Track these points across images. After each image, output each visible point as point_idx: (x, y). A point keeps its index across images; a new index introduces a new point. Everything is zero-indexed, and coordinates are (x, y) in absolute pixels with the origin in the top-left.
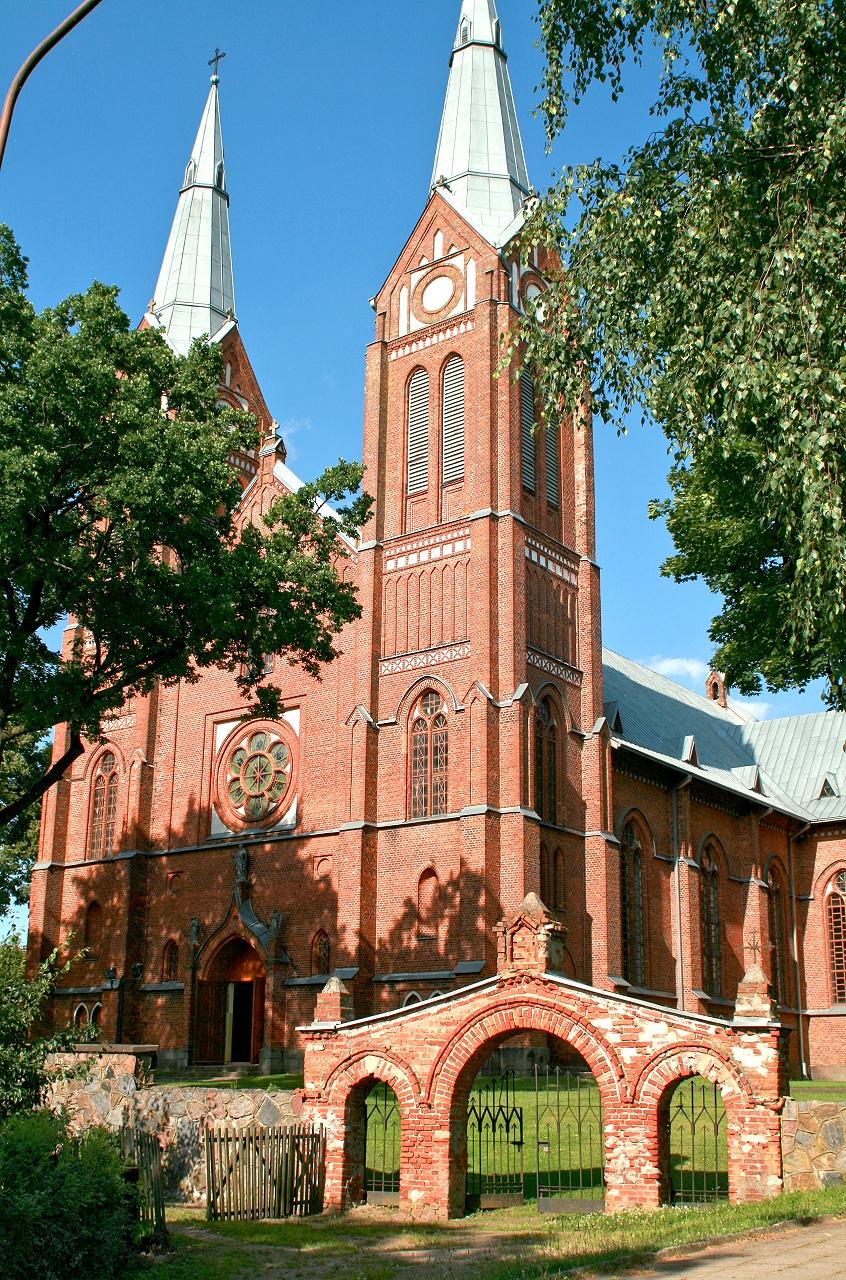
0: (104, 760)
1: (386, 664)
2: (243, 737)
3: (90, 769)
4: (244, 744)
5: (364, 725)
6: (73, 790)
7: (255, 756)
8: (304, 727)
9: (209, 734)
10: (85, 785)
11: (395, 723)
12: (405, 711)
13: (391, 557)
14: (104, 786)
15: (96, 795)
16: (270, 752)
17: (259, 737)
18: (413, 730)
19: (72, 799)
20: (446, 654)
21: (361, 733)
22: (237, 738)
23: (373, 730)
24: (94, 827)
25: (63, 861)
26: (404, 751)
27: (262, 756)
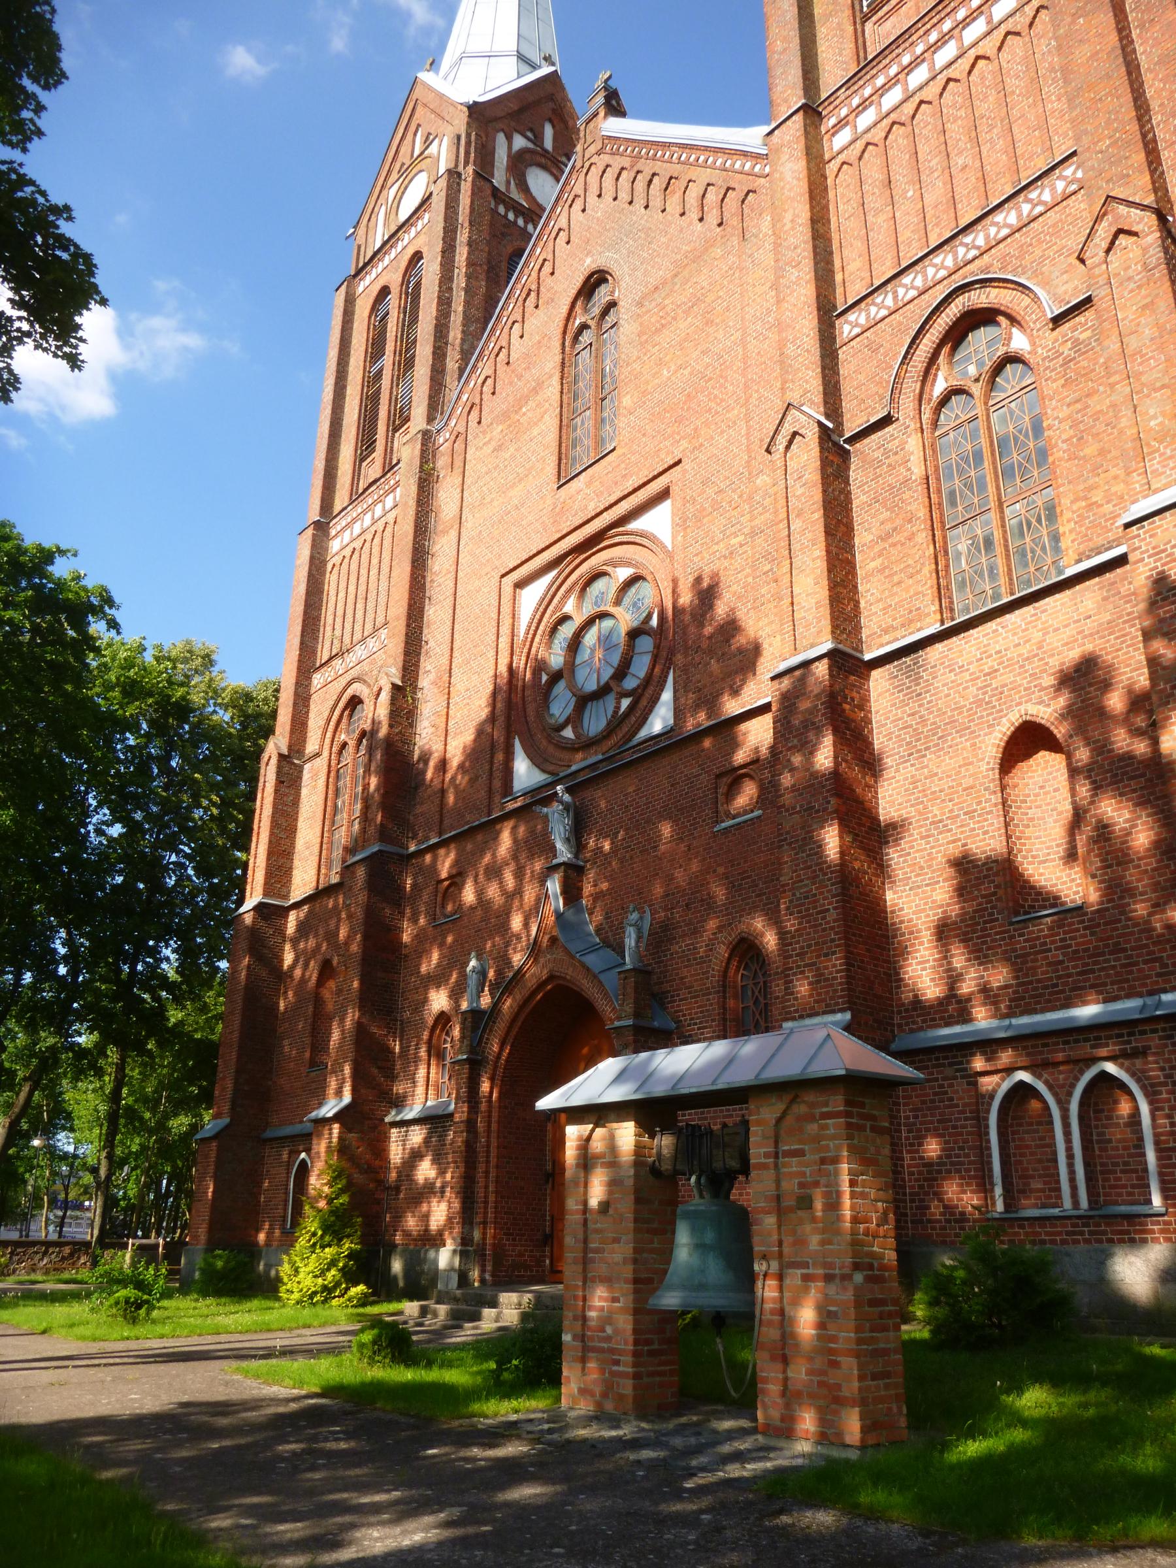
0: (351, 716)
1: (852, 317)
3: (329, 735)
4: (569, 607)
5: (811, 434)
6: (306, 775)
7: (590, 622)
8: (681, 523)
10: (321, 764)
11: (886, 421)
12: (911, 386)
13: (841, 124)
14: (348, 756)
15: (338, 777)
16: (618, 602)
17: (600, 585)
18: (935, 424)
19: (304, 792)
20: (1009, 217)
21: (807, 456)
22: (555, 601)
23: (835, 452)
24: (332, 832)
25: (286, 897)
26: (918, 471)
27: (603, 615)
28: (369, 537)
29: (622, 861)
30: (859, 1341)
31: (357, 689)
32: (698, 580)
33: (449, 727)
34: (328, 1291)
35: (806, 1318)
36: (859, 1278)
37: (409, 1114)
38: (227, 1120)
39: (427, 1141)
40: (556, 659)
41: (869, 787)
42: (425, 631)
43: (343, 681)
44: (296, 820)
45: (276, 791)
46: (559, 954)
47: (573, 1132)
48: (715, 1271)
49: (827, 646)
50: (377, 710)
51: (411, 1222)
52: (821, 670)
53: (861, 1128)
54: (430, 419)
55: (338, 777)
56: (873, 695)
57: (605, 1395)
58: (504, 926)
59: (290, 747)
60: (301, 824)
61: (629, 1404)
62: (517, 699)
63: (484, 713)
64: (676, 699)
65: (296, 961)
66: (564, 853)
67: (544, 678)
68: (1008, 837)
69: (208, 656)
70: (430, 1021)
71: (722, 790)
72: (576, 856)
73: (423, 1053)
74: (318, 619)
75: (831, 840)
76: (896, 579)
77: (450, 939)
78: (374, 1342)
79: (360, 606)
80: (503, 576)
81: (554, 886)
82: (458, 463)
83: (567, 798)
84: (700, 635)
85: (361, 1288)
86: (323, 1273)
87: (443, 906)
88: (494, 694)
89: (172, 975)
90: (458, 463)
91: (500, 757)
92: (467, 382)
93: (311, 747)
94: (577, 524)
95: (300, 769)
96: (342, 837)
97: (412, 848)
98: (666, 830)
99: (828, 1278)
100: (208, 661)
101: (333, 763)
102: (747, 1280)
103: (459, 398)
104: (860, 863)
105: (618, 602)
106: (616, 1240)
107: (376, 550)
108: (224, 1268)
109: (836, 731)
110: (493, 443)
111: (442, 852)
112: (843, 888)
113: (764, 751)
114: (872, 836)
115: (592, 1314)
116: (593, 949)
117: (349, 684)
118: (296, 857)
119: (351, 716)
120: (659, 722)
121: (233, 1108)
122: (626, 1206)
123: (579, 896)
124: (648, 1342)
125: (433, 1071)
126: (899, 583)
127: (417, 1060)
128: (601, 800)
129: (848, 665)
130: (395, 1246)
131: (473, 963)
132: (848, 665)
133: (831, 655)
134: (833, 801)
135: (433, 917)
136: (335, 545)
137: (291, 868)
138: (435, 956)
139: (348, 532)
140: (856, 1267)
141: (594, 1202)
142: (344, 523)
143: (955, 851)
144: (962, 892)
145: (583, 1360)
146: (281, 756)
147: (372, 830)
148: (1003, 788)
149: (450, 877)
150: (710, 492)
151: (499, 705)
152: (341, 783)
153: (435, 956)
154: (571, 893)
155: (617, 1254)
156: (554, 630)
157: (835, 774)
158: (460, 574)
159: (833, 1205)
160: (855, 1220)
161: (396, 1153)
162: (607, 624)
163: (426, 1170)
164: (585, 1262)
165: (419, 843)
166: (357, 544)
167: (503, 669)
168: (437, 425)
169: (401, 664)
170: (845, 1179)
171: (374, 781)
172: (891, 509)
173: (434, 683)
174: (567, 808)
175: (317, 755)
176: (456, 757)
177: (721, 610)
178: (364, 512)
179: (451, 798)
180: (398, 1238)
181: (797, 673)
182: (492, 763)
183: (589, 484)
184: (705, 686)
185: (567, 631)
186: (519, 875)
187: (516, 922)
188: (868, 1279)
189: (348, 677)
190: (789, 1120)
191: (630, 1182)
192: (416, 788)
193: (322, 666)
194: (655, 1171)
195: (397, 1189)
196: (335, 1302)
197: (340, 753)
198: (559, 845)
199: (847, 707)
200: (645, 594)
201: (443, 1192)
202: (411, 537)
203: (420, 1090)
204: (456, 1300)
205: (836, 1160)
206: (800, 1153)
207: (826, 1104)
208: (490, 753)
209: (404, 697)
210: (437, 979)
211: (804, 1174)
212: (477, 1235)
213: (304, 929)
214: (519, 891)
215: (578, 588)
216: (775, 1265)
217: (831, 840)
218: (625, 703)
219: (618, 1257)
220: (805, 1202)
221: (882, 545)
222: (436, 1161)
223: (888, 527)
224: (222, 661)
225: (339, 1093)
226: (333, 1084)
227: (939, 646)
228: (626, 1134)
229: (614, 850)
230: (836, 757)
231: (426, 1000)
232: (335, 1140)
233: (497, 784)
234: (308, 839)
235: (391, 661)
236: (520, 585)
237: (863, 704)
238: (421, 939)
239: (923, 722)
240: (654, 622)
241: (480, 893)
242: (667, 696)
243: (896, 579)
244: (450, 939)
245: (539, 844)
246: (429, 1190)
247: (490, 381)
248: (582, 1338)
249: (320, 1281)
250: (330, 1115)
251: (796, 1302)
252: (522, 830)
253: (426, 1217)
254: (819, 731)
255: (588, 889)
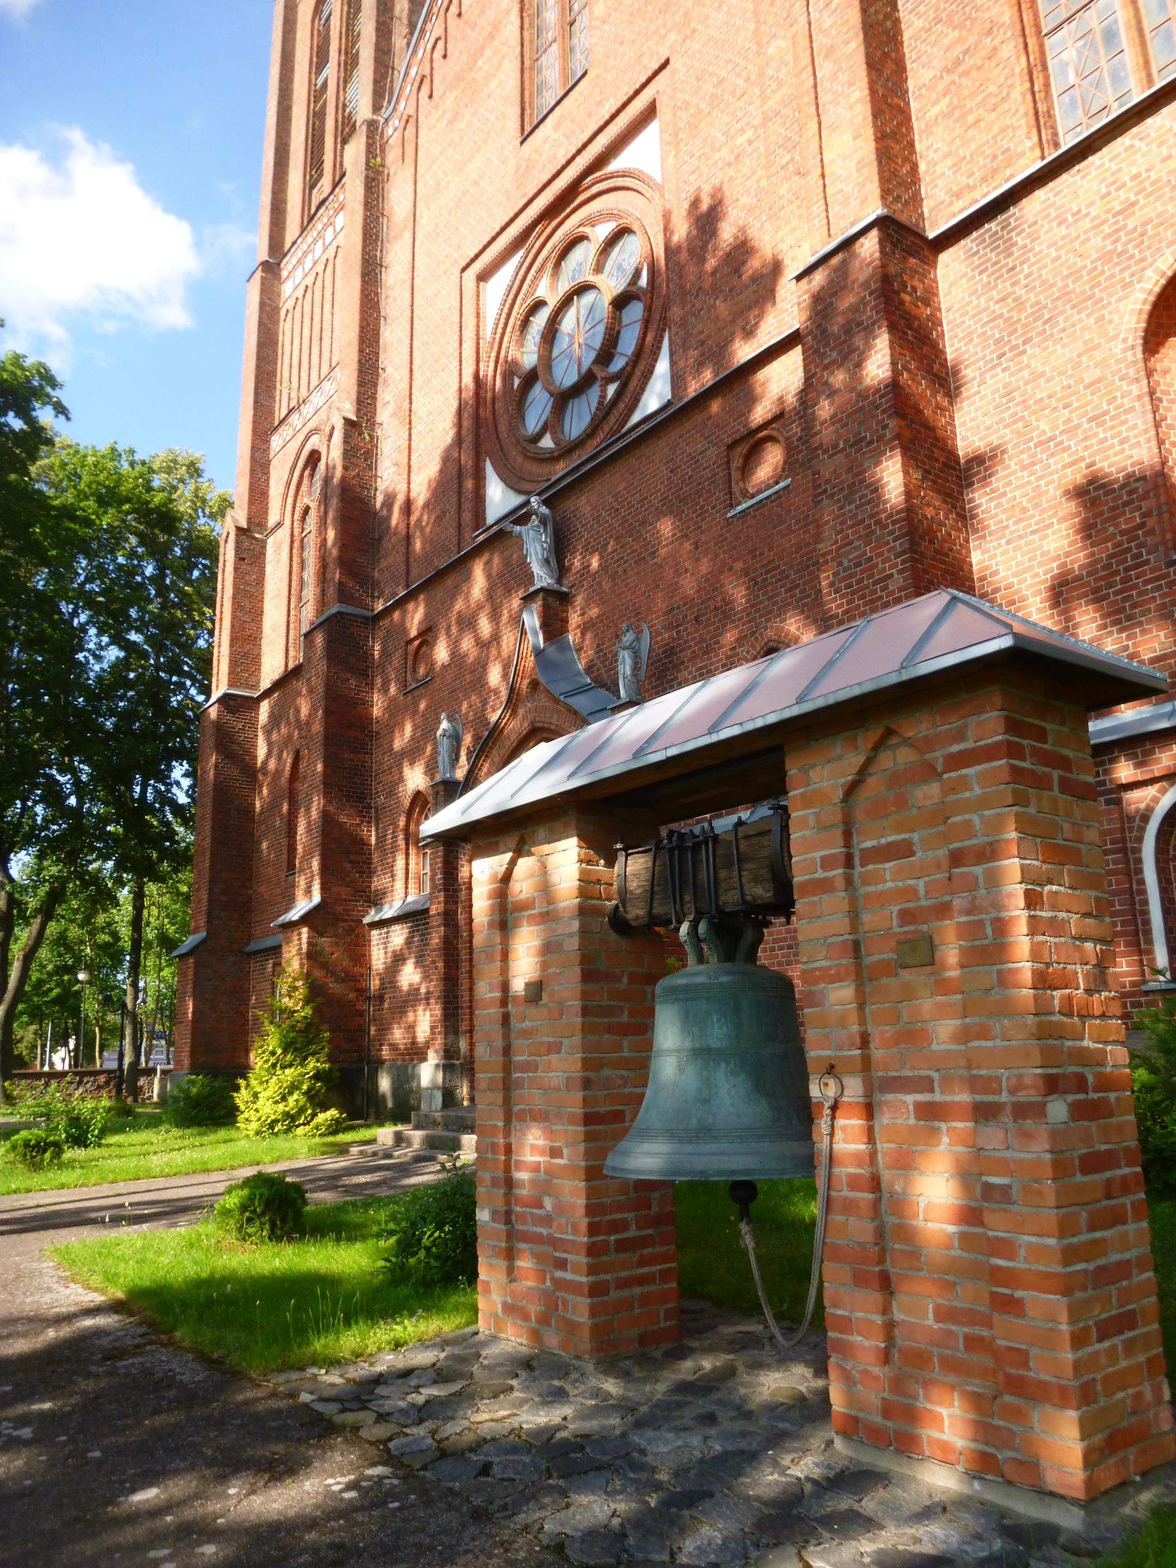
2: (541, 269)
3: (290, 500)
8: (672, 141)
9: (469, 309)
10: (283, 534)
15: (302, 548)
16: (599, 268)
19: (269, 568)
24: (299, 609)
25: (255, 687)
28: (320, 268)
29: (613, 577)
30: (1070, 1255)
31: (315, 442)
32: (695, 203)
33: (411, 462)
34: (291, 1120)
35: (934, 1194)
36: (1058, 1109)
37: (388, 912)
38: (204, 934)
39: (409, 942)
40: (529, 357)
41: (943, 409)
42: (382, 357)
43: (301, 437)
44: (262, 601)
45: (236, 569)
46: (542, 700)
47: (482, 872)
48: (732, 1098)
49: (875, 210)
50: (334, 454)
51: (398, 1035)
52: (869, 246)
53: (1042, 783)
54: (377, 108)
55: (302, 548)
56: (942, 287)
57: (544, 1320)
58: (479, 682)
59: (249, 520)
60: (267, 606)
61: (585, 1342)
62: (486, 413)
63: (449, 436)
64: (673, 363)
65: (269, 755)
66: (542, 577)
67: (517, 381)
68: (1161, 443)
69: (192, 464)
70: (407, 802)
71: (737, 463)
72: (559, 581)
73: (401, 843)
74: (273, 373)
75: (892, 476)
76: (971, 119)
77: (422, 706)
78: (243, 1208)
79: (315, 350)
80: (464, 270)
81: (532, 619)
82: (410, 152)
83: (544, 510)
84: (700, 275)
85: (333, 1113)
86: (284, 1099)
87: (414, 670)
88: (459, 412)
89: (183, 799)
90: (410, 152)
91: (469, 484)
92: (415, 51)
93: (272, 520)
94: (544, 180)
95: (263, 544)
96: (309, 613)
97: (380, 606)
98: (666, 527)
99: (984, 1113)
100: (194, 470)
101: (297, 531)
102: (797, 1115)
103: (407, 74)
104: (933, 509)
105: (599, 268)
106: (555, 1048)
107: (328, 284)
108: (198, 1094)
109: (892, 328)
110: (448, 116)
111: (411, 606)
112: (913, 543)
113: (791, 400)
114: (951, 476)
115: (522, 1176)
116: (582, 690)
117: (307, 438)
118: (264, 642)
119: (312, 476)
120: (655, 397)
121: (209, 922)
122: (568, 988)
123: (564, 630)
124: (615, 1227)
125: (412, 861)
126: (977, 122)
127: (394, 849)
128: (583, 504)
129: (906, 242)
130: (381, 1062)
131: (445, 725)
132: (906, 242)
133: (881, 223)
134: (893, 423)
135: (403, 684)
136: (287, 289)
137: (259, 655)
138: (408, 729)
139: (300, 269)
140: (1052, 1085)
141: (518, 985)
142: (294, 260)
143: (1077, 475)
144: (1088, 531)
145: (510, 1255)
146: (239, 529)
147: (331, 592)
148: (1149, 374)
149: (421, 634)
150: (707, 87)
151: (465, 424)
152: (305, 554)
153: (408, 729)
154: (553, 627)
155: (558, 1070)
156: (525, 323)
157: (894, 386)
158: (417, 281)
159: (989, 949)
160: (1043, 981)
161: (378, 958)
162: (589, 298)
163: (409, 975)
164: (507, 1086)
165: (386, 601)
166: (309, 281)
167: (468, 380)
168: (385, 113)
169: (354, 397)
170: (1015, 891)
171: (331, 534)
172: (961, 26)
173: (394, 415)
174: (543, 521)
175: (279, 525)
176: (421, 491)
177: (727, 233)
178: (315, 241)
179: (418, 545)
180: (385, 1053)
181: (835, 261)
182: (460, 493)
183: (556, 128)
184: (709, 337)
185: (540, 320)
186: (495, 617)
187: (494, 676)
188: (1080, 1111)
189: (305, 431)
190: (874, 785)
191: (573, 944)
192: (380, 539)
193: (281, 422)
194: (618, 922)
195: (381, 998)
196: (300, 1131)
197: (303, 519)
198: (537, 569)
199: (907, 298)
200: (630, 254)
201: (427, 999)
202: (359, 248)
203: (399, 884)
204: (435, 1124)
205: (990, 853)
206: (903, 850)
207: (960, 736)
208: (458, 485)
209: (359, 432)
210: (412, 753)
211: (912, 893)
212: (463, 1045)
213: (275, 719)
214: (496, 637)
215: (550, 265)
216: (854, 1089)
217: (892, 476)
218: (612, 389)
219: (556, 1077)
220: (920, 952)
221: (947, 79)
222: (419, 963)
223: (957, 51)
224: (209, 469)
225: (308, 891)
226: (302, 882)
227: (1040, 194)
228: (564, 859)
229: (603, 567)
230: (894, 363)
231: (401, 779)
232: (304, 946)
233: (467, 516)
234: (273, 621)
235: (344, 396)
236: (483, 277)
237: (929, 297)
238: (395, 712)
239: (1020, 304)
240: (643, 281)
241: (454, 646)
242: (662, 367)
243: (971, 119)
244: (422, 706)
245: (513, 576)
246: (412, 998)
247: (441, 44)
248: (507, 1217)
249: (281, 1107)
250: (296, 918)
251: (906, 1163)
252: (496, 560)
253: (411, 1028)
254: (869, 332)
255: (574, 619)
